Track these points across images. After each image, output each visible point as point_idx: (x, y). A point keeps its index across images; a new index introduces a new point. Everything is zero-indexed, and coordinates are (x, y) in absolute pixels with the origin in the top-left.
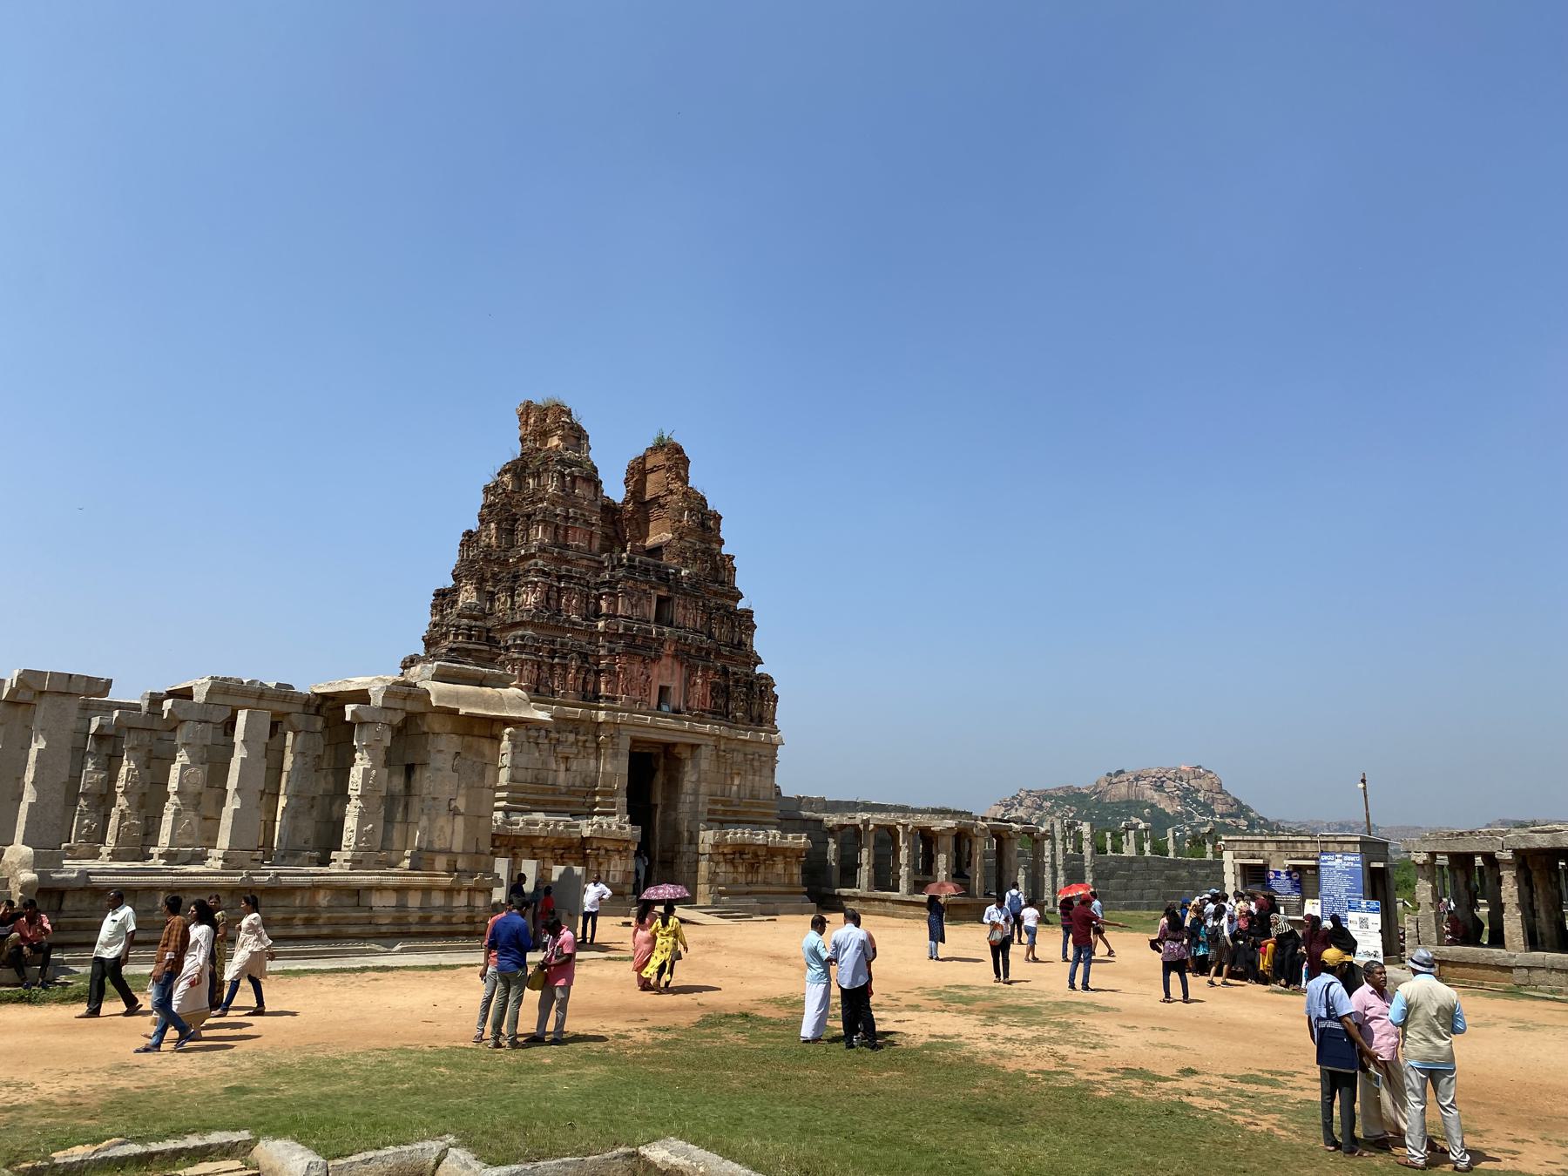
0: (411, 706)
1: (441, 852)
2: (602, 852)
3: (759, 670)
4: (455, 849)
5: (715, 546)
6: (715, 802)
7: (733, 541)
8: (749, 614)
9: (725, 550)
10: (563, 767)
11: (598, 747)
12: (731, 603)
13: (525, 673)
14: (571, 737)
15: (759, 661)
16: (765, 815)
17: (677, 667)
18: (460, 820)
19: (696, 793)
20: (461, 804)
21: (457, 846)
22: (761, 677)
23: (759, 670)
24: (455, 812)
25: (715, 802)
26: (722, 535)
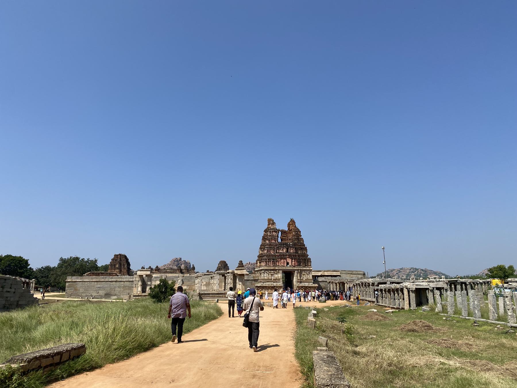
7: (303, 235)
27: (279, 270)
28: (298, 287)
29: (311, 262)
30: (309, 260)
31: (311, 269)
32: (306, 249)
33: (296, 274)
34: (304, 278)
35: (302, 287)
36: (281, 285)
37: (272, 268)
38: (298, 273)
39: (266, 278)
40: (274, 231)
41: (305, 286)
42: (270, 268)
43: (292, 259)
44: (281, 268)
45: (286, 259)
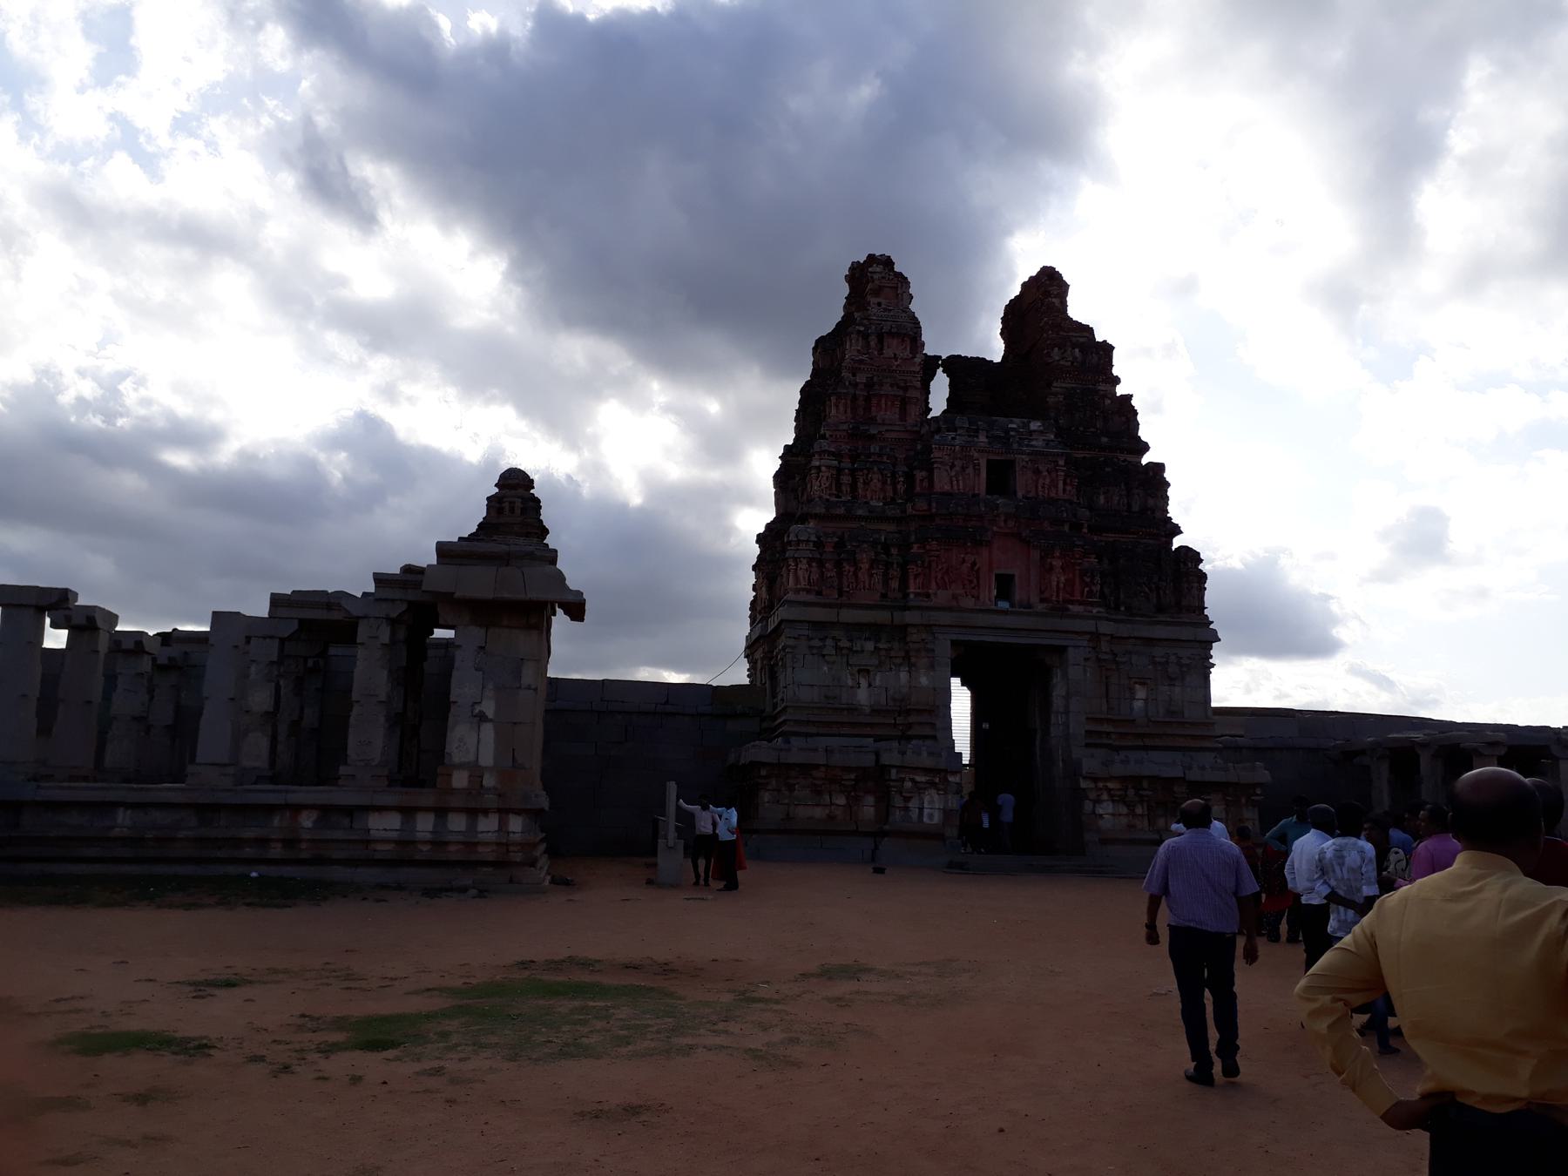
0: (411, 595)
1: (461, 766)
2: (908, 784)
3: (1177, 542)
4: (482, 762)
5: (1102, 387)
8: (1160, 468)
9: (1120, 390)
10: (864, 683)
11: (907, 657)
12: (1130, 458)
13: (800, 573)
14: (870, 646)
15: (1176, 530)
16: (1193, 737)
18: (488, 731)
19: (1067, 712)
20: (489, 708)
21: (487, 759)
23: (1177, 542)
24: (482, 718)
26: (1115, 372)
42: (848, 616)
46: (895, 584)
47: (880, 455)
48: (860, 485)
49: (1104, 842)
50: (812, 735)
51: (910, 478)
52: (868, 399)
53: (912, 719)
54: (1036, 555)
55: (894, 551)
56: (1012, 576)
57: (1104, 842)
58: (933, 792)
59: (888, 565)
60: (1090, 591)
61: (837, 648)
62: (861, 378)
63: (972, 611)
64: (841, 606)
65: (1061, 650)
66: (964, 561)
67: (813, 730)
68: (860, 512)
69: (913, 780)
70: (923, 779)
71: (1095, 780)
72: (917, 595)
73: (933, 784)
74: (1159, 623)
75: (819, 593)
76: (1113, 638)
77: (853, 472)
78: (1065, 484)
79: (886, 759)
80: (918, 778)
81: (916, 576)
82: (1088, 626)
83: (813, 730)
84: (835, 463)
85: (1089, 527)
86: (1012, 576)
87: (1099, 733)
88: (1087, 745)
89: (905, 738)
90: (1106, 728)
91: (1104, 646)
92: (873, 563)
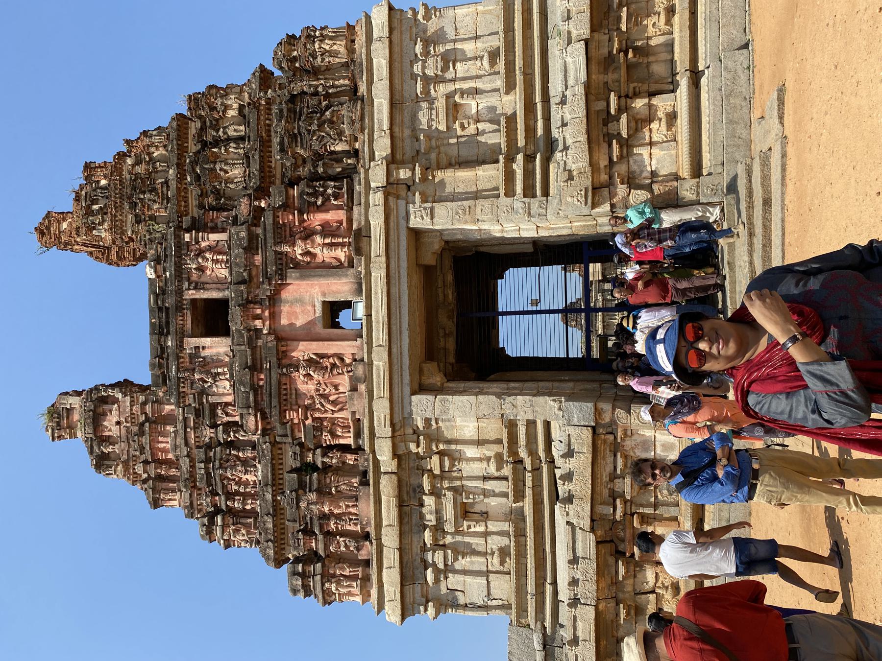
6: (509, 176)
8: (194, 100)
13: (343, 591)
14: (429, 501)
17: (285, 294)
22: (281, 68)
25: (509, 176)
27: (400, 424)
28: (598, 191)
29: (310, 35)
30: (299, 55)
31: (380, 18)
32: (206, 103)
33: (446, 220)
34: (489, 100)
35: (599, 127)
36: (582, 439)
37: (390, 514)
38: (435, 196)
39: (503, 588)
40: (96, 419)
41: (591, 92)
42: (390, 539)
43: (285, 266)
44: (381, 409)
45: (284, 339)
46: (350, 459)
47: (207, 461)
48: (242, 490)
49: (697, 171)
50: (555, 593)
51: (228, 426)
52: (159, 463)
53: (523, 453)
54: (292, 274)
55: (310, 458)
56: (324, 303)
57: (697, 171)
58: (628, 443)
59: (327, 468)
60: (336, 197)
61: (438, 546)
62: (139, 469)
63: (371, 364)
64: (379, 539)
65: (416, 234)
66: (308, 375)
67: (549, 588)
68: (269, 497)
69: (613, 477)
70: (610, 459)
71: (596, 189)
72: (358, 435)
73: (616, 448)
74: (369, 90)
75: (367, 563)
76: (393, 161)
77: (230, 496)
78: (215, 230)
79: (586, 523)
80: (609, 468)
81: (333, 435)
82: (377, 198)
83: (549, 588)
84: (219, 519)
85: (259, 199)
86: (324, 302)
87: (529, 175)
88: (546, 193)
89: (551, 462)
90: (518, 167)
91: (404, 174)
92: (323, 492)
